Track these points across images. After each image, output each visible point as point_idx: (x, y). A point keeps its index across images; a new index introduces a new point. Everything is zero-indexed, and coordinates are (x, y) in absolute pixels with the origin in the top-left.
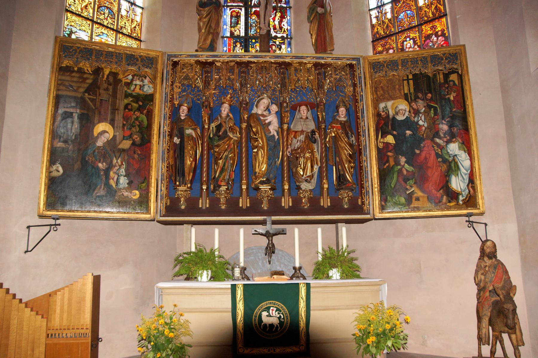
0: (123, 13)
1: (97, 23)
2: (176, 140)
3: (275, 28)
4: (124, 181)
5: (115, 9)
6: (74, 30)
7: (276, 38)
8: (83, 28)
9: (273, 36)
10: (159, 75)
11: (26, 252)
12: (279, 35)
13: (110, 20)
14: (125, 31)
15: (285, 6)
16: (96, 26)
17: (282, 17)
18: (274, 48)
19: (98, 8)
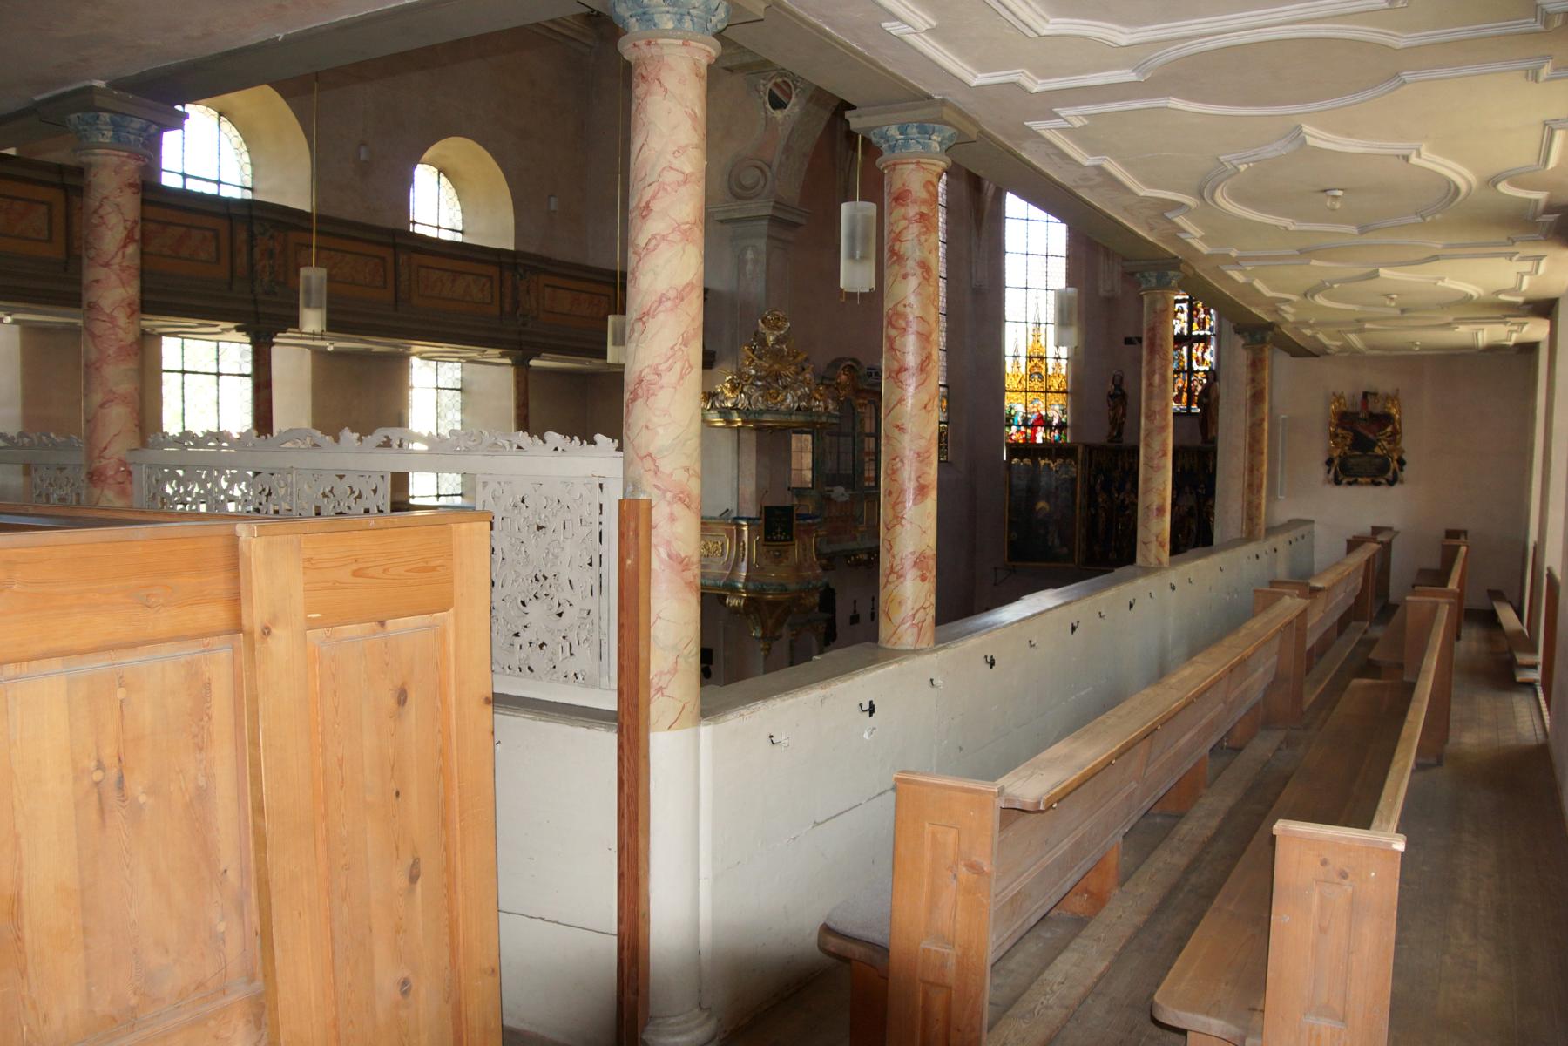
0: (1050, 372)
1: (1030, 391)
2: (1093, 511)
3: (1197, 361)
4: (1057, 542)
5: (1043, 373)
6: (1013, 405)
7: (1198, 371)
8: (1019, 401)
9: (1195, 369)
10: (1079, 462)
11: (995, 584)
12: (1202, 368)
13: (1040, 384)
14: (1053, 389)
15: (1209, 333)
16: (1029, 394)
17: (1205, 348)
18: (1195, 383)
19: (1030, 376)
